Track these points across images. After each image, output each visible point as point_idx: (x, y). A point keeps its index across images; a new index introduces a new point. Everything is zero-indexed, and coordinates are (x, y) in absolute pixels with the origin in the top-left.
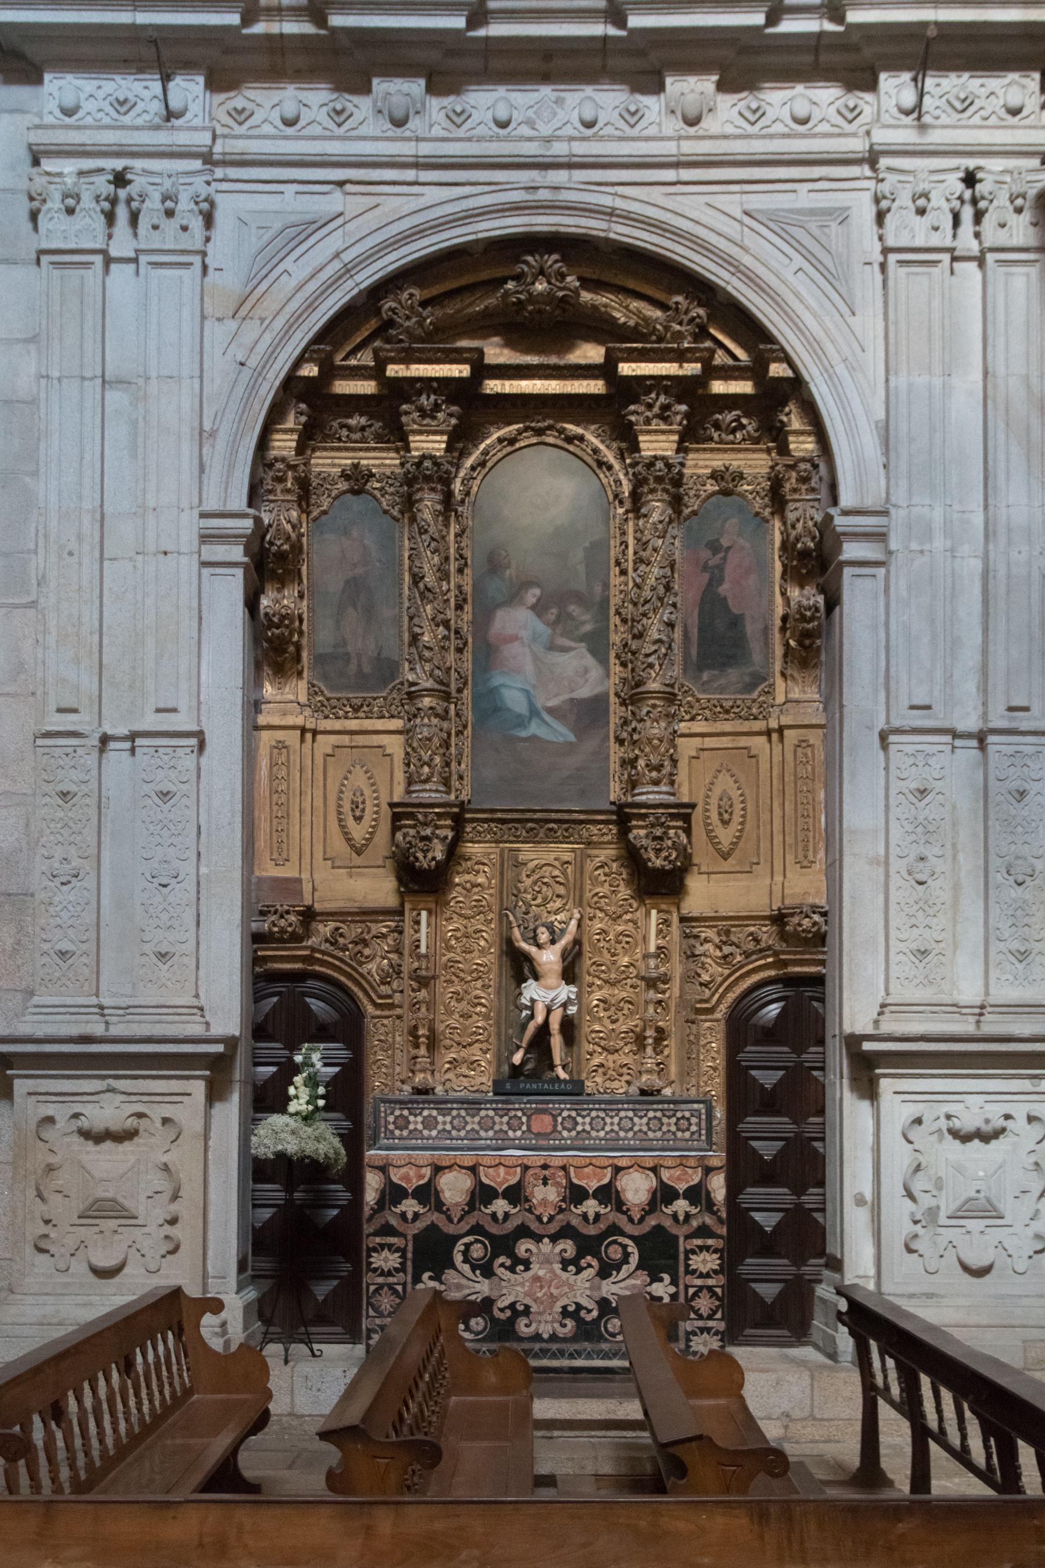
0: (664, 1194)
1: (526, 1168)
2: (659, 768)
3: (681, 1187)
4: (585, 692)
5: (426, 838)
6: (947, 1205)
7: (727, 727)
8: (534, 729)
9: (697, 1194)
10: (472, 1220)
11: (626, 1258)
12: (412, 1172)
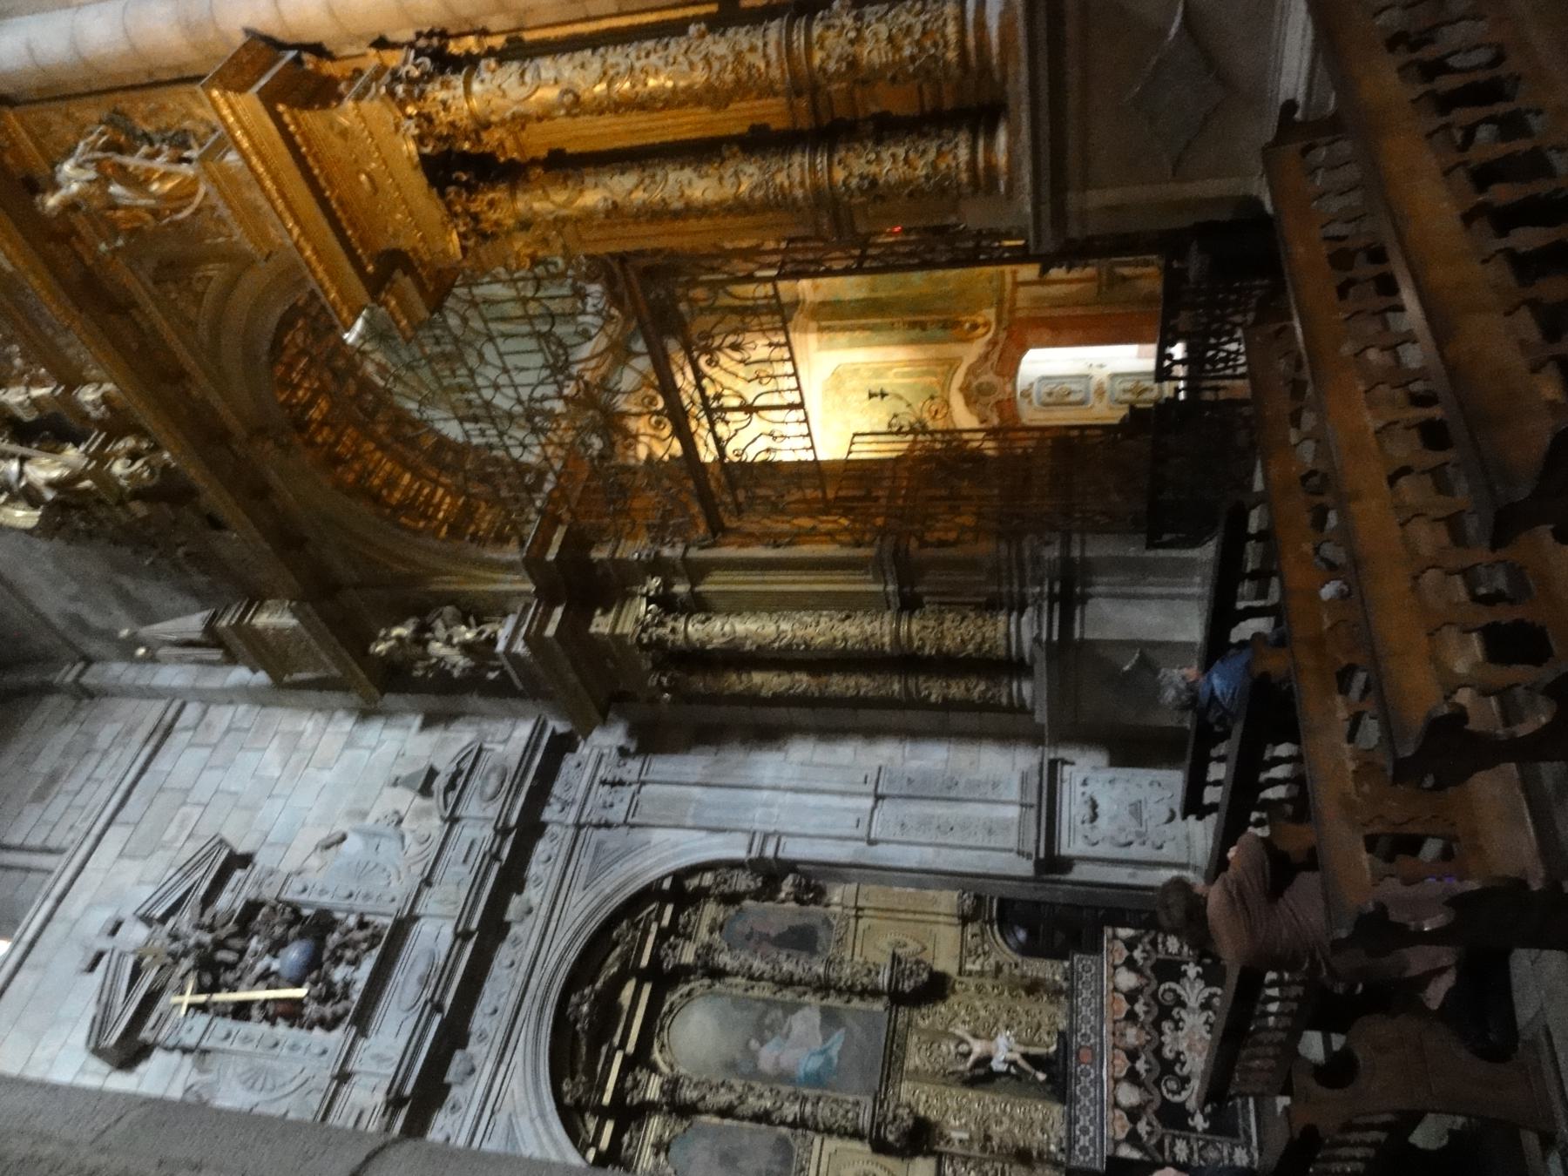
0: (1130, 964)
1: (1115, 1046)
2: (870, 971)
3: (1126, 953)
4: (816, 1018)
5: (895, 1118)
6: (1132, 826)
7: (850, 939)
8: (834, 1052)
9: (1131, 944)
10: (1151, 1086)
11: (1174, 991)
12: (1118, 1124)
